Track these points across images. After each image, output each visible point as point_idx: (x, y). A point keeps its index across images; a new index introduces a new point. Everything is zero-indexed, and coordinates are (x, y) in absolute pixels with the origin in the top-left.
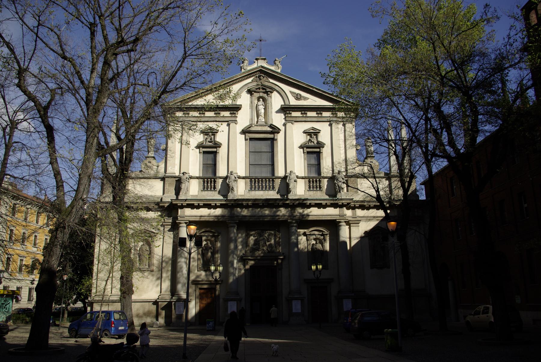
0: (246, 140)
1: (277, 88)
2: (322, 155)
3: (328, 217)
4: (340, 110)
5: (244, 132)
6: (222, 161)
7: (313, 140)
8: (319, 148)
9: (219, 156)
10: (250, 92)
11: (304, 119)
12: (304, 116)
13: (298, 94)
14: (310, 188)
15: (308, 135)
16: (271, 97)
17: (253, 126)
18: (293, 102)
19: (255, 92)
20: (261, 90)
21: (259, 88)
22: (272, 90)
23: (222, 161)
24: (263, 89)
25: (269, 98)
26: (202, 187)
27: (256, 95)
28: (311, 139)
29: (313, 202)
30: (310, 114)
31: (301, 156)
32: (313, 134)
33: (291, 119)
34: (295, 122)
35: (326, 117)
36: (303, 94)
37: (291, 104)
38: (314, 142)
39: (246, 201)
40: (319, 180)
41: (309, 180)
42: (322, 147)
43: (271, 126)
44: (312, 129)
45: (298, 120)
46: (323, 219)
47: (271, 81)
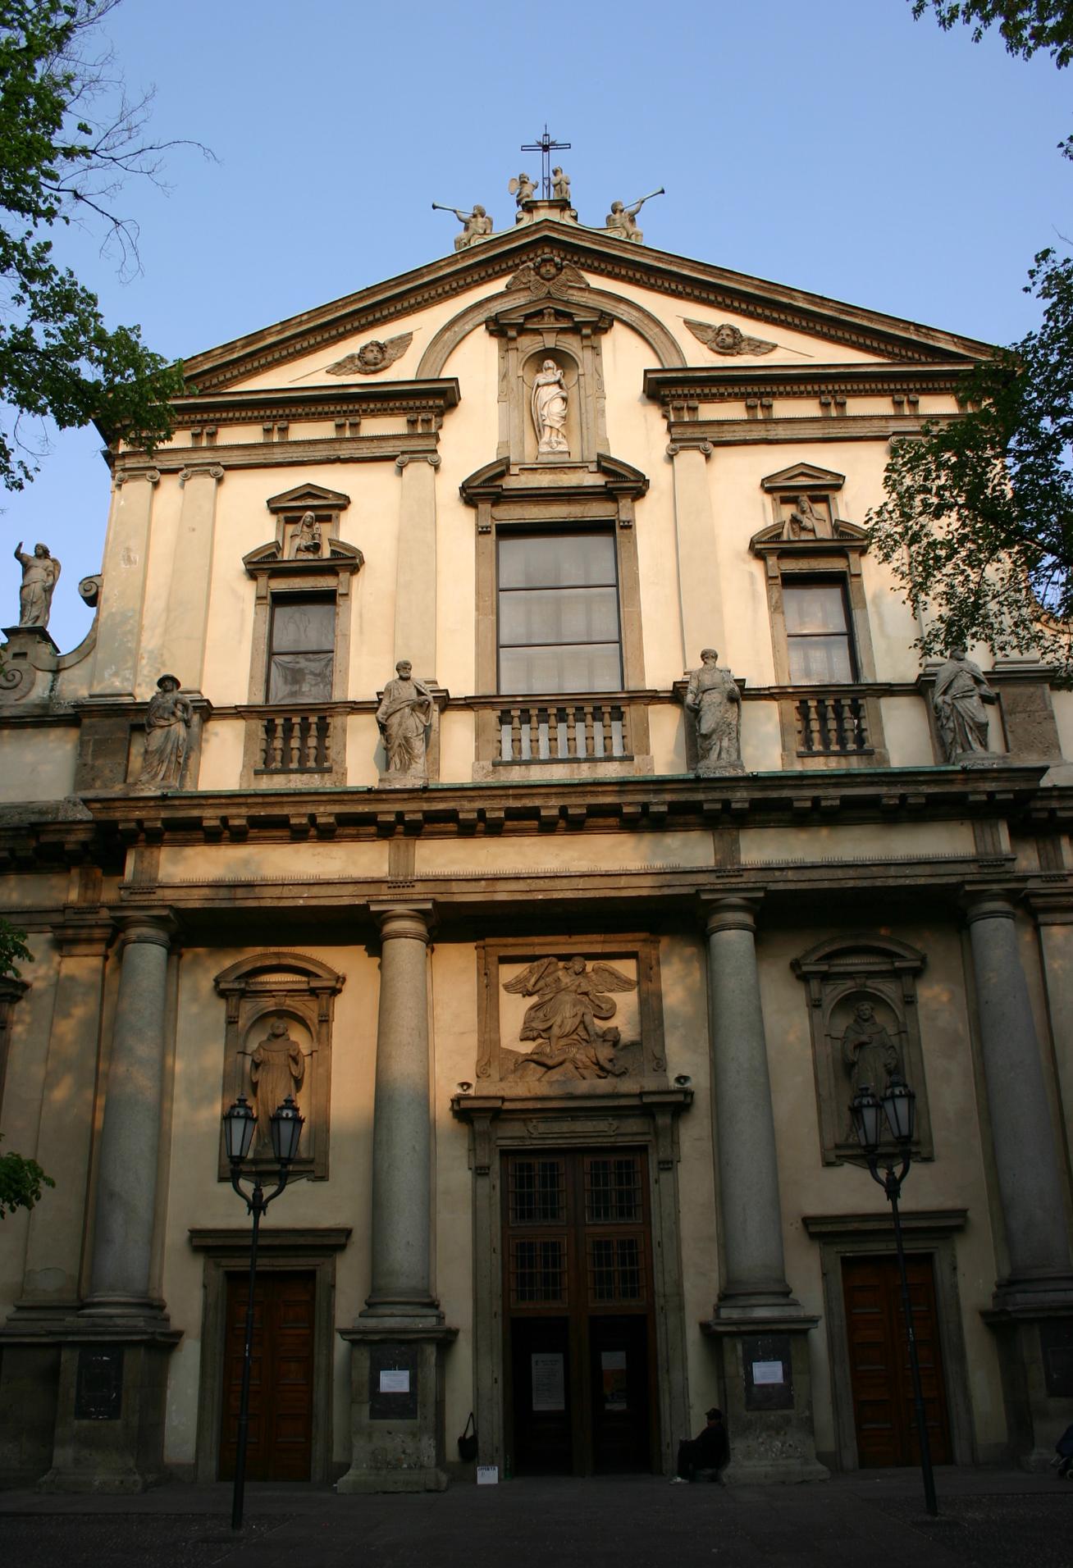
0: (482, 532)
1: (621, 311)
2: (861, 587)
3: (919, 870)
4: (932, 384)
5: (475, 493)
6: (361, 632)
7: (807, 523)
8: (841, 553)
9: (349, 609)
10: (499, 328)
11: (758, 432)
13: (722, 327)
14: (808, 741)
15: (785, 501)
16: (596, 350)
17: (514, 470)
18: (698, 356)
19: (522, 330)
20: (549, 322)
21: (540, 314)
22: (602, 324)
23: (361, 632)
24: (559, 314)
25: (588, 354)
26: (259, 757)
27: (529, 344)
28: (800, 516)
29: (833, 792)
30: (783, 408)
31: (754, 595)
32: (804, 498)
33: (697, 433)
34: (718, 444)
35: (863, 418)
36: (749, 328)
37: (690, 365)
38: (813, 531)
39: (471, 799)
40: (854, 701)
41: (803, 702)
42: (854, 549)
43: (606, 465)
45: (728, 437)
46: (891, 882)
47: (596, 281)
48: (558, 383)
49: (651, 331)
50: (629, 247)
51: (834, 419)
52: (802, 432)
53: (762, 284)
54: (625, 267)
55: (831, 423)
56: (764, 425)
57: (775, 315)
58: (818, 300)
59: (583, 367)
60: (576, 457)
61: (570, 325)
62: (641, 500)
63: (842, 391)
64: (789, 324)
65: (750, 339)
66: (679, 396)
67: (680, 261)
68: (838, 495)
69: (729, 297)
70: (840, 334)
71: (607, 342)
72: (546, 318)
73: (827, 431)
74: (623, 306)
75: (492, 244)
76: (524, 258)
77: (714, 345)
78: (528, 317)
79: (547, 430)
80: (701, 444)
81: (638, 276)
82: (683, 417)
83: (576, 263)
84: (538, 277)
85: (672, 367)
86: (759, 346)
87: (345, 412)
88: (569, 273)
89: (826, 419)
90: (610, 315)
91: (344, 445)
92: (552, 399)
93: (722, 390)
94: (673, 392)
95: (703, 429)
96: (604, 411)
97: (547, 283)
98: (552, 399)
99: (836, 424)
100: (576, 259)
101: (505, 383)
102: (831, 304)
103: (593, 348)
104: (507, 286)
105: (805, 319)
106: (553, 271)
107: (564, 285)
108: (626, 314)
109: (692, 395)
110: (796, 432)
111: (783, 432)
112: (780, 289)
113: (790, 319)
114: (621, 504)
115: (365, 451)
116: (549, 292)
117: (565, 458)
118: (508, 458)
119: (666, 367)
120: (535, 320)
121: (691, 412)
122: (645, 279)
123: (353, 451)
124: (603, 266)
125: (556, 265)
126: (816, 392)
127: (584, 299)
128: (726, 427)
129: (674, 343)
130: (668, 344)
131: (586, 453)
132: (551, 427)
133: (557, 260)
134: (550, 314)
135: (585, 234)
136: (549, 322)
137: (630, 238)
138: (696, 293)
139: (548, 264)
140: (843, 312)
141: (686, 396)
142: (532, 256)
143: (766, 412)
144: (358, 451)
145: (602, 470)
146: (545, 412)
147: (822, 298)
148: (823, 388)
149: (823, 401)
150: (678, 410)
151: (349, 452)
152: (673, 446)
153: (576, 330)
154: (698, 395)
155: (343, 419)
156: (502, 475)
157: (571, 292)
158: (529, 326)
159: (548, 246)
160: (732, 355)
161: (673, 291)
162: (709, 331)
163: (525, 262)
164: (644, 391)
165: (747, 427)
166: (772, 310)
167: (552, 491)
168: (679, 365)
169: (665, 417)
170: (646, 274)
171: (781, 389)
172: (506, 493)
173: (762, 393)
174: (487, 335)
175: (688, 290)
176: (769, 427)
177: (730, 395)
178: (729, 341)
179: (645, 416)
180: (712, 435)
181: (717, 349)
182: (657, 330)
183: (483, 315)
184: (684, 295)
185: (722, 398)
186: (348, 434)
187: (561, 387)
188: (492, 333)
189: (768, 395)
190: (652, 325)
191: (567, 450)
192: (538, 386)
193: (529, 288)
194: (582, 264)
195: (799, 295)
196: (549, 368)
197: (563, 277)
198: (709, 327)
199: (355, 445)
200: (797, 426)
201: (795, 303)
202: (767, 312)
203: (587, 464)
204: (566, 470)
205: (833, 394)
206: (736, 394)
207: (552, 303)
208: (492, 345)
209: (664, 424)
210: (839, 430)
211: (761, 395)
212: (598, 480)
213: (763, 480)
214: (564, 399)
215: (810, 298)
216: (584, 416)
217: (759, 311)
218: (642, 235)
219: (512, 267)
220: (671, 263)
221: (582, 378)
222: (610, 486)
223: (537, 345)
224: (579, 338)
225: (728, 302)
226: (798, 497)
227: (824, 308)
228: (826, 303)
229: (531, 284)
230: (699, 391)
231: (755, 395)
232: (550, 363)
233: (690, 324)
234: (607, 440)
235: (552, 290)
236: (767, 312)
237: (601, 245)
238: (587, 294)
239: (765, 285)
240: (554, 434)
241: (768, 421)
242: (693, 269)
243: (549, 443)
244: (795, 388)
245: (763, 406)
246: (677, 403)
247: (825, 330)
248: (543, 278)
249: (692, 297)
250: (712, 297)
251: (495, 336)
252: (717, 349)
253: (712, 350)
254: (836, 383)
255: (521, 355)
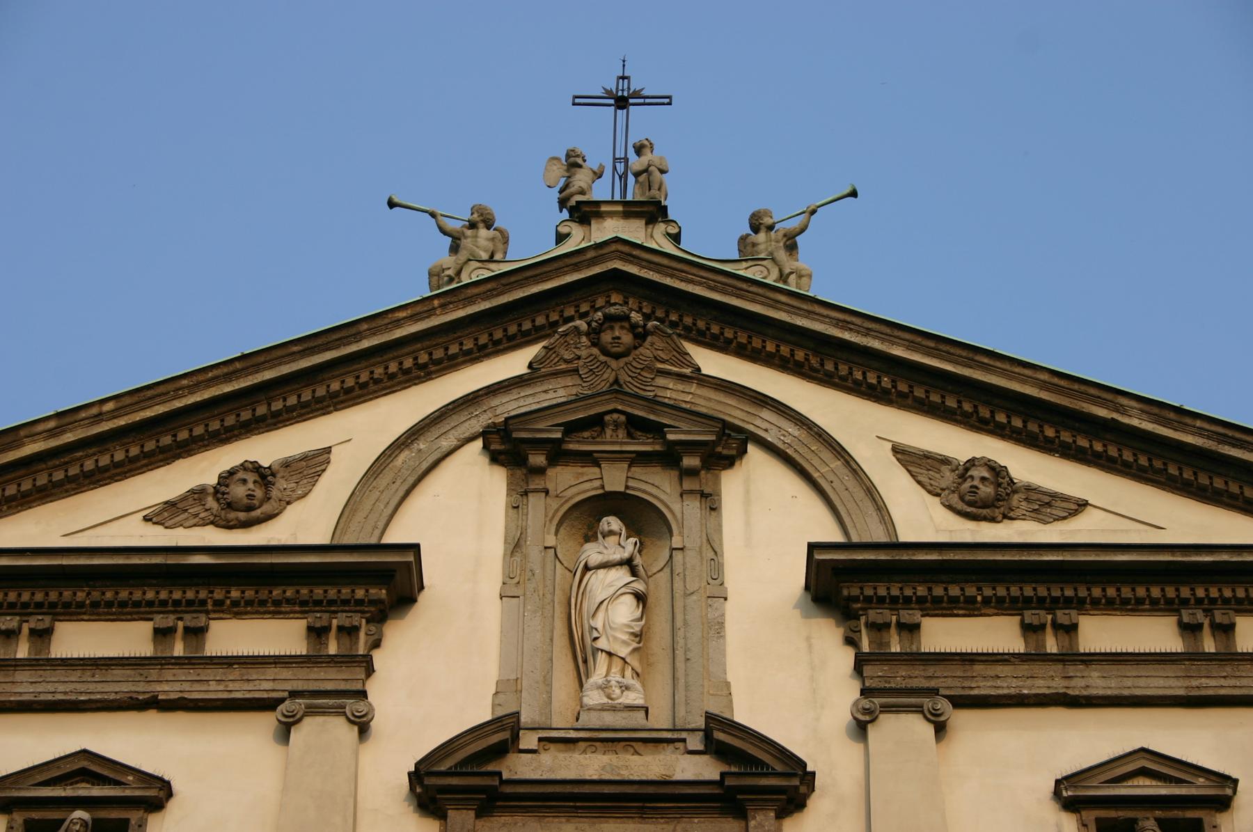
11: (1046, 681)
12: (1052, 646)
13: (972, 462)
16: (711, 501)
17: (529, 740)
19: (558, 454)
20: (614, 440)
21: (596, 422)
24: (636, 426)
33: (918, 677)
37: (905, 536)
44: (1144, 772)
45: (984, 688)
47: (712, 363)
48: (628, 563)
49: (825, 467)
50: (783, 298)
51: (1209, 658)
52: (1142, 682)
53: (1056, 380)
54: (774, 338)
55: (1204, 667)
56: (1060, 666)
57: (1083, 442)
58: (1172, 415)
59: (681, 534)
60: (660, 719)
61: (658, 448)
62: (797, 817)
63: (1226, 601)
64: (1111, 460)
65: (1029, 488)
66: (881, 600)
67: (888, 331)
68: (1222, 819)
69: (987, 403)
70: (1219, 483)
71: (731, 484)
72: (609, 432)
73: (1195, 683)
74: (766, 414)
75: (504, 281)
76: (570, 312)
77: (954, 499)
78: (571, 428)
79: (602, 659)
80: (927, 703)
81: (800, 355)
82: (888, 644)
83: (673, 325)
84: (595, 351)
85: (866, 539)
86: (1048, 504)
87: (177, 603)
88: (659, 344)
89: (1192, 657)
90: (740, 430)
91: (168, 674)
92: (614, 597)
93: (971, 591)
94: (869, 592)
95: (931, 671)
96: (721, 624)
97: (614, 363)
98: (614, 597)
99: (1214, 669)
100: (674, 318)
101: (517, 558)
102: (1199, 423)
103: (704, 496)
104: (530, 366)
105: (1144, 452)
106: (627, 338)
107: (649, 368)
108: (774, 431)
109: (907, 600)
110: (1129, 682)
111: (1100, 682)
112: (1092, 391)
113: (1113, 451)
114: (752, 823)
115: (213, 686)
116: (616, 381)
117: (638, 719)
118: (517, 715)
119: (855, 539)
120: (586, 434)
121: (905, 634)
122: (814, 362)
123: (186, 686)
124: (729, 334)
125: (633, 327)
126: (1169, 602)
127: (688, 398)
128: (978, 668)
129: (871, 491)
130: (859, 494)
131: (681, 712)
132: (610, 654)
133: (636, 317)
134: (617, 425)
135: (695, 271)
136: (614, 440)
137: (785, 282)
138: (919, 393)
139: (617, 326)
140: (1223, 439)
141: (894, 600)
142: (584, 308)
143: (1065, 640)
144: (197, 687)
145: (714, 748)
146: (598, 622)
147: (1179, 411)
148: (1185, 592)
149: (1186, 619)
150: (878, 628)
151: (177, 687)
152: (866, 703)
153: (669, 457)
154: (921, 601)
155: (172, 617)
156: (500, 751)
157: (661, 381)
158: (572, 447)
159: (618, 291)
160: (993, 520)
161: (871, 386)
162: (945, 469)
163: (571, 319)
164: (807, 588)
165: (1024, 669)
166: (1076, 431)
167: (607, 790)
168: (880, 536)
169: (850, 641)
170: (816, 352)
171: (1097, 592)
172: (508, 789)
173: (1055, 600)
174: (484, 460)
175: (903, 387)
176: (1071, 670)
177: (987, 601)
178: (987, 490)
179: (808, 639)
180: (950, 682)
181: (961, 506)
182: (837, 464)
183: (477, 423)
184: (894, 397)
185: (970, 608)
186: (179, 650)
187: (634, 572)
188: (495, 458)
189: (1068, 603)
190: (826, 455)
191: (640, 702)
192: (587, 568)
193: (576, 371)
194: (688, 329)
195: (1133, 403)
196: (611, 533)
197: (645, 351)
198: (945, 461)
199: (192, 674)
200: (1130, 670)
201: (1125, 420)
202: (1066, 437)
203: (684, 735)
204: (637, 745)
205: (1208, 605)
206: (1001, 601)
207: (623, 402)
208: (496, 481)
209: (846, 657)
210: (1222, 682)
211: (1052, 604)
212: (703, 769)
213: (1058, 782)
214: (640, 598)
215: (1156, 410)
216: (681, 633)
217: (1050, 432)
218: (810, 276)
219: (542, 327)
220: (867, 333)
221: (678, 556)
222: (729, 782)
223: (587, 486)
224: (674, 474)
225: (985, 412)
226: (1135, 821)
227: (1183, 431)
228: (1188, 420)
229: (581, 363)
230: (921, 591)
231: (1041, 603)
232: (614, 523)
233: (906, 456)
234: (728, 685)
235: (623, 377)
236: (1066, 437)
237: (725, 293)
238: (693, 388)
239: (1062, 383)
240: (616, 669)
241: (1073, 658)
242: (912, 346)
243: (604, 687)
244: (1126, 592)
245: (1057, 627)
246: (874, 615)
247: (1188, 475)
248: (605, 352)
249: (910, 401)
250: (951, 403)
251: (502, 464)
252: (961, 506)
253: (950, 507)
254: (1213, 583)
255: (554, 504)
